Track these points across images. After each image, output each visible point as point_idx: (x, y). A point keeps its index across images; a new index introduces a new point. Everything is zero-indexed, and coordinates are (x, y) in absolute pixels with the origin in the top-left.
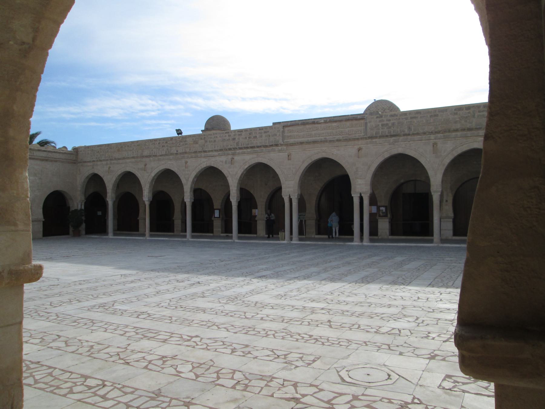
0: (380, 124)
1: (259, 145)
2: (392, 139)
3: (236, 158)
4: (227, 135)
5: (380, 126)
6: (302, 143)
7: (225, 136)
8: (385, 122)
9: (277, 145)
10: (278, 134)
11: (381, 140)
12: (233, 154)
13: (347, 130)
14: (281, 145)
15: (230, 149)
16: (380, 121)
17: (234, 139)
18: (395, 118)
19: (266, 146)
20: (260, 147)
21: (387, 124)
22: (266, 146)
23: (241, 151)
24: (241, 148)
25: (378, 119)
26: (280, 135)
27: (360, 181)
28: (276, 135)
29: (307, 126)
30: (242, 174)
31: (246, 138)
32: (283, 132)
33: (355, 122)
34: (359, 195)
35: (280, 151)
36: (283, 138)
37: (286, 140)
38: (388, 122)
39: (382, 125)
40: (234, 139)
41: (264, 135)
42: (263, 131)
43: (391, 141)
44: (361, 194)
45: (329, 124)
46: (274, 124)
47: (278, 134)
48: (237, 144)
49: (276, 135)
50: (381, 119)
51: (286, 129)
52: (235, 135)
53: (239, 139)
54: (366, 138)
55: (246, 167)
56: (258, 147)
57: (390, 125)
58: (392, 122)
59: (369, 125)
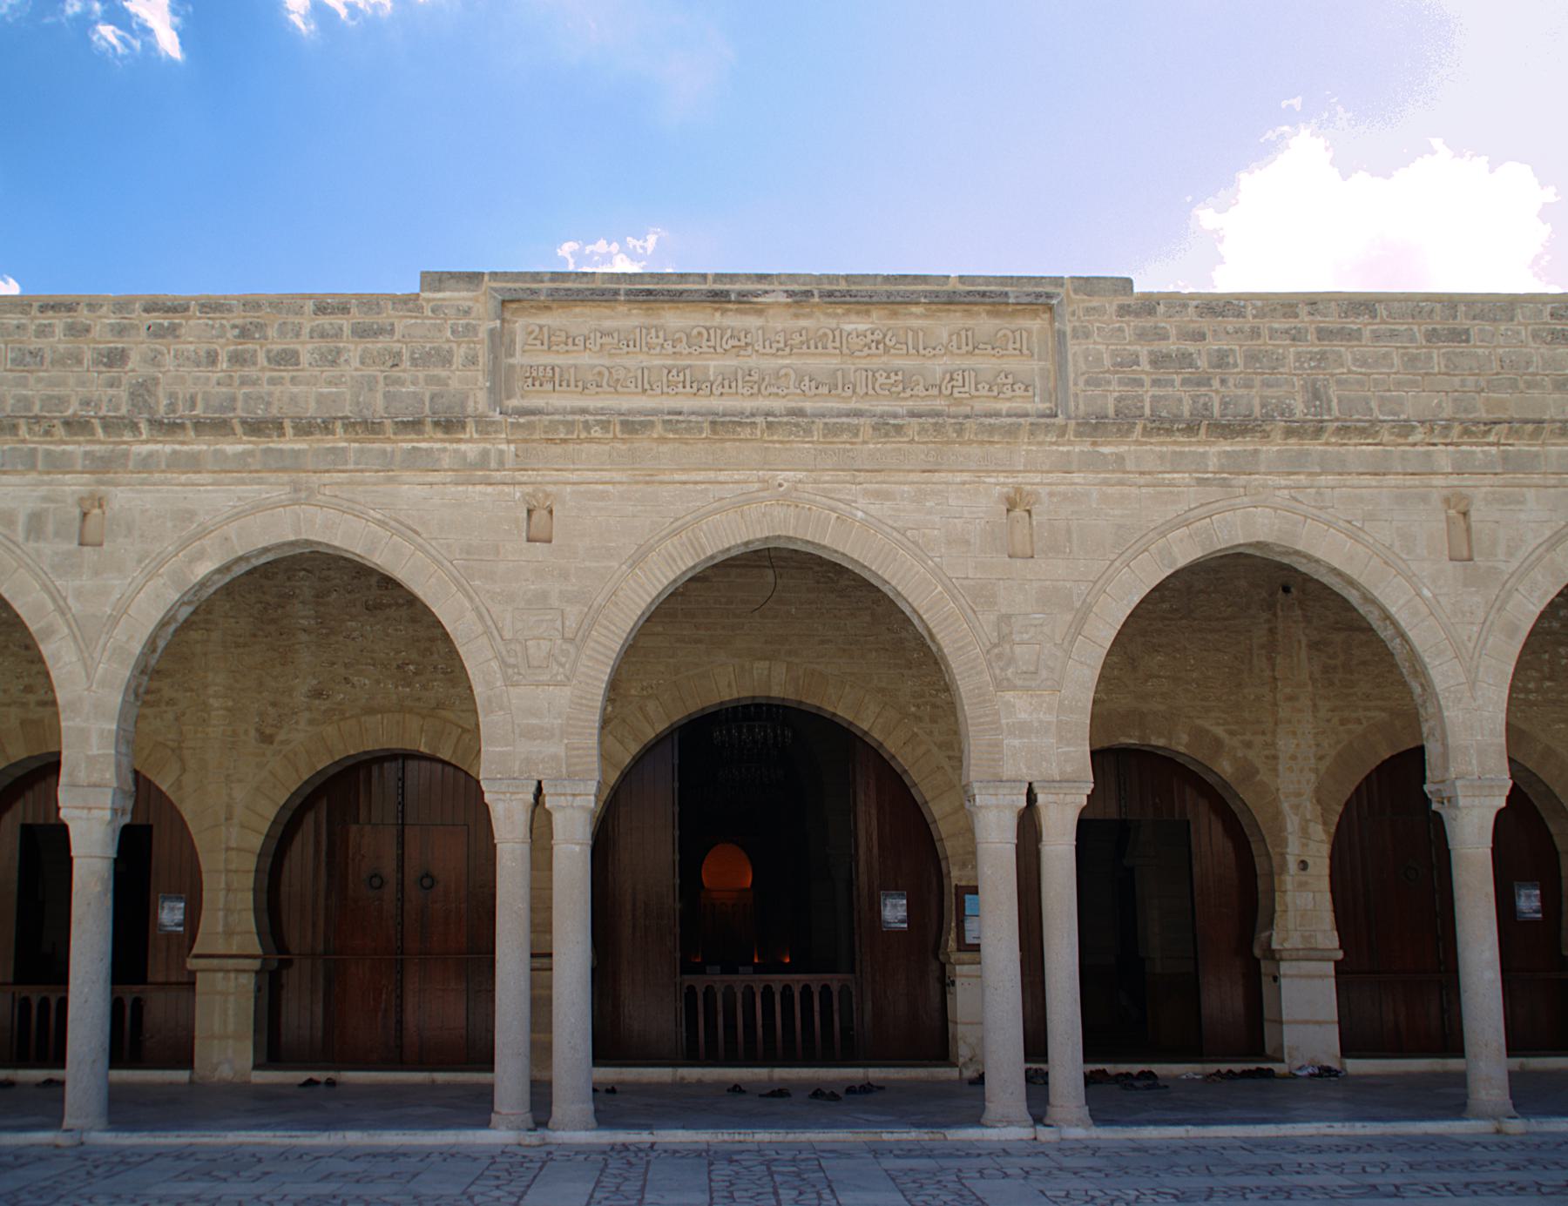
0: (1143, 351)
1: (311, 410)
3: (123, 497)
4: (59, 322)
7: (43, 331)
8: (1172, 346)
9: (450, 425)
10: (460, 353)
12: (102, 465)
13: (938, 366)
14: (485, 426)
15: (77, 426)
16: (1142, 335)
17: (115, 358)
18: (1231, 323)
21: (1185, 359)
22: (369, 427)
23: (165, 448)
24: (169, 428)
25: (1131, 325)
28: (446, 360)
29: (673, 319)
30: (163, 624)
31: (212, 358)
32: (500, 342)
33: (984, 324)
36: (501, 381)
38: (1191, 347)
39: (1158, 360)
40: (115, 358)
41: (353, 350)
42: (345, 323)
46: (435, 280)
47: (460, 353)
48: (142, 391)
49: (446, 360)
50: (1147, 322)
52: (121, 331)
53: (154, 360)
55: (203, 569)
56: (305, 428)
57: (1202, 363)
58: (1213, 345)
59: (1073, 347)
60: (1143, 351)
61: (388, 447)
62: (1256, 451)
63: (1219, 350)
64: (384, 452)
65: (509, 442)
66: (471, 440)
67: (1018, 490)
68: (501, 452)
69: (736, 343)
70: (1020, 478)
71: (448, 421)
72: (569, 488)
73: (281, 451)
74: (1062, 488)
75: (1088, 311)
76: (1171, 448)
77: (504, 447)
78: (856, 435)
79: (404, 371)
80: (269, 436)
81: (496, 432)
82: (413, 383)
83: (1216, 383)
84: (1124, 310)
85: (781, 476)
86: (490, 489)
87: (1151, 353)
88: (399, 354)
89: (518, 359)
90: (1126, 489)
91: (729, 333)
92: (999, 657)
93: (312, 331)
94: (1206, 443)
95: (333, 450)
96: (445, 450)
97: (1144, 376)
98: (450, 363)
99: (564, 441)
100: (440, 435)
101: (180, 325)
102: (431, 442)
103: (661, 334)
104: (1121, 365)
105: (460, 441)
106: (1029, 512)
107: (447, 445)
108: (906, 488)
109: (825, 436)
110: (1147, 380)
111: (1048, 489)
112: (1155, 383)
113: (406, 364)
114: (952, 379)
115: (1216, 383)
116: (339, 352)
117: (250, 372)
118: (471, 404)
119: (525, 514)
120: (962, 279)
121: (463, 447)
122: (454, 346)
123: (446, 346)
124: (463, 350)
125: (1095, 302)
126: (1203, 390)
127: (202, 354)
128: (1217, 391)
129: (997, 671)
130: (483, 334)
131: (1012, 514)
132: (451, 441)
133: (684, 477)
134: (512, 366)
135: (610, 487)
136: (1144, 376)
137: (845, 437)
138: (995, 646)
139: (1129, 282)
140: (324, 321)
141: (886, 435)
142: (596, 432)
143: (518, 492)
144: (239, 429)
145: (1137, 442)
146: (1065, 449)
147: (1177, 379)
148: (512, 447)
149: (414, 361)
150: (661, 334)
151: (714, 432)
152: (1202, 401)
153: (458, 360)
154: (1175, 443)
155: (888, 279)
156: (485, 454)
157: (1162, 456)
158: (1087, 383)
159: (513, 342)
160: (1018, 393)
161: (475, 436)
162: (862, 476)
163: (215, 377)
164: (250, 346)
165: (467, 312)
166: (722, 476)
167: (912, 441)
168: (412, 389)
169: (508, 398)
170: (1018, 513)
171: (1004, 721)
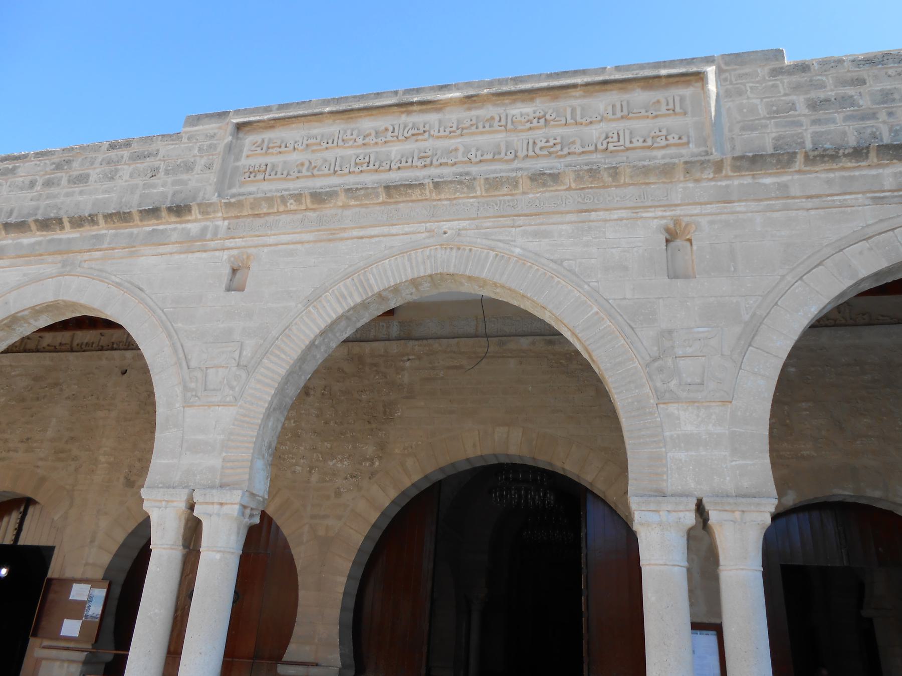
0: (800, 100)
5: (802, 108)
8: (830, 92)
9: (179, 210)
11: (820, 178)
13: (595, 132)
14: (206, 209)
16: (797, 88)
19: (121, 217)
20: (92, 220)
21: (845, 101)
26: (209, 167)
27: (688, 420)
28: (188, 167)
29: (367, 124)
31: (32, 184)
33: (639, 97)
35: (190, 244)
38: (850, 91)
39: (814, 105)
41: (125, 170)
42: (126, 153)
43: (889, 183)
51: (249, 140)
54: (718, 166)
56: (78, 222)
60: (800, 100)
61: (135, 231)
63: (881, 90)
64: (132, 234)
65: (224, 219)
66: (196, 221)
67: (677, 222)
68: (217, 228)
69: (416, 132)
70: (678, 212)
71: (178, 206)
72: (266, 250)
73: (60, 240)
74: (724, 217)
75: (740, 76)
76: (838, 174)
77: (220, 223)
78: (516, 186)
79: (159, 179)
80: (54, 230)
81: (214, 212)
82: (163, 186)
83: (882, 116)
84: (777, 72)
85: (446, 226)
86: (204, 255)
87: (808, 100)
88: (158, 169)
89: (244, 162)
90: (793, 214)
91: (410, 125)
92: (660, 370)
93: (103, 160)
94: (879, 166)
95: (96, 237)
96: (175, 229)
97: (802, 119)
98: (192, 169)
99: (268, 214)
100: (174, 219)
101: (19, 167)
102: (169, 225)
103: (355, 133)
104: (777, 112)
105: (188, 221)
106: (690, 241)
107: (178, 226)
108: (564, 227)
109: (487, 190)
111: (709, 218)
112: (815, 122)
113: (162, 174)
114: (607, 137)
115: (882, 116)
116: (117, 171)
117: (54, 190)
118: (201, 194)
119: (227, 271)
120: (618, 68)
121: (189, 226)
122: (198, 159)
123: (192, 160)
124: (204, 161)
125: (747, 70)
126: (869, 123)
127: (27, 182)
128: (884, 122)
129: (659, 384)
130: (221, 148)
131: (672, 244)
132: (181, 223)
133: (361, 233)
134: (237, 168)
135: (299, 246)
136: (802, 119)
137: (505, 190)
138: (655, 360)
139: (778, 54)
140: (113, 154)
141: (544, 185)
142: (292, 205)
143: (225, 255)
144: (33, 227)
145: (799, 172)
146: (724, 183)
147: (839, 117)
148: (226, 223)
149: (167, 172)
150: (355, 133)
151: (389, 195)
152: (869, 131)
153: (198, 168)
154: (843, 169)
156: (204, 230)
157: (829, 182)
158: (743, 129)
159: (241, 151)
160: (671, 141)
161: (199, 217)
162: (521, 221)
163: (30, 195)
164: (59, 174)
165: (212, 137)
166: (394, 230)
167: (569, 189)
168: (161, 189)
169: (230, 188)
170: (678, 243)
171: (667, 434)
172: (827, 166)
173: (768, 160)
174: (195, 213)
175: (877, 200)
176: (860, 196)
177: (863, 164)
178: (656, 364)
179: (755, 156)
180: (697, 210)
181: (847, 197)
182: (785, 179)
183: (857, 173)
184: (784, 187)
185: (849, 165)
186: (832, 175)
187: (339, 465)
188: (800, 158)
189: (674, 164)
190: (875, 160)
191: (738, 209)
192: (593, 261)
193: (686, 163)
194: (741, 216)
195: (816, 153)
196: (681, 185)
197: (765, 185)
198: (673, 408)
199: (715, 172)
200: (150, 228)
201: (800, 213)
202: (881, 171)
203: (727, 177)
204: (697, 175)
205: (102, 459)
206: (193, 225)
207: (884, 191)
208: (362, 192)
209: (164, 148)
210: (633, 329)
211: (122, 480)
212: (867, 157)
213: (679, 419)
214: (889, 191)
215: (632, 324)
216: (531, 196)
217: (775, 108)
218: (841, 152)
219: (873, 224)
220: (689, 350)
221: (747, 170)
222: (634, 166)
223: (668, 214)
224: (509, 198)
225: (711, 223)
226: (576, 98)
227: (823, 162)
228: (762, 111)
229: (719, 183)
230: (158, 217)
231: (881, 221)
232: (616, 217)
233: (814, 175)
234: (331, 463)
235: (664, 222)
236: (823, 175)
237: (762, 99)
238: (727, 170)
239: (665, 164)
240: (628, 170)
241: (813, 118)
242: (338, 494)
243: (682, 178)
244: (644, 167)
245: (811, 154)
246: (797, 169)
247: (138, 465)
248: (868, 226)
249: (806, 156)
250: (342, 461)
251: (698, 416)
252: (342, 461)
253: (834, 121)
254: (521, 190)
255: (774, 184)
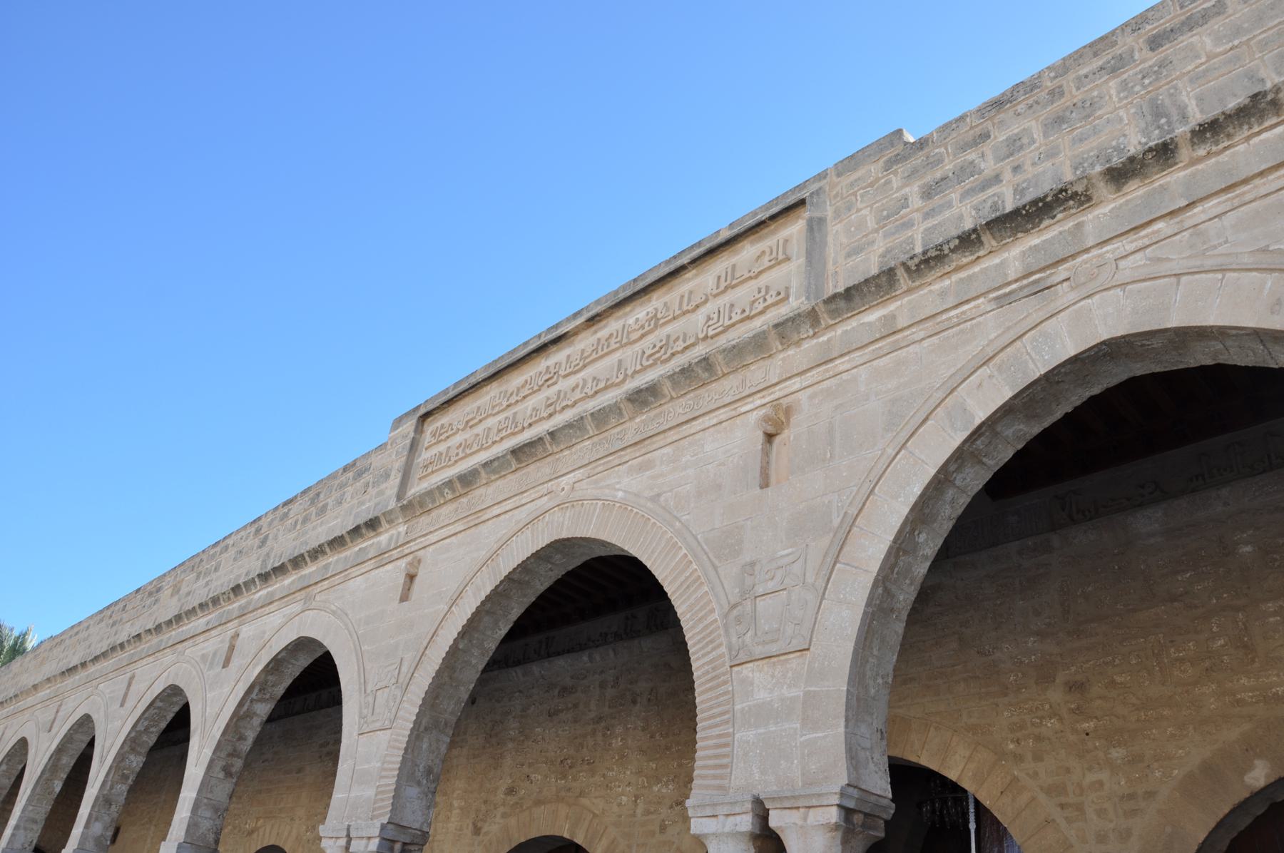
2: (1012, 257)
6: (467, 480)
11: (934, 291)
27: (761, 685)
34: (746, 823)
35: (382, 558)
37: (413, 491)
44: (762, 815)
45: (612, 326)
62: (1079, 226)
66: (386, 531)
70: (777, 392)
76: (955, 277)
78: (621, 414)
83: (1007, 175)
92: (738, 620)
104: (888, 217)
108: (665, 451)
109: (597, 427)
110: (917, 216)
119: (401, 579)
120: (731, 226)
138: (734, 607)
143: (402, 563)
145: (909, 291)
146: (824, 338)
151: (519, 460)
154: (959, 269)
155: (668, 262)
157: (943, 294)
167: (672, 398)
172: (939, 272)
173: (865, 290)
174: (385, 525)
175: (1002, 301)
176: (981, 300)
177: (981, 253)
178: (735, 612)
179: (848, 290)
180: (796, 384)
181: (966, 307)
182: (892, 307)
183: (977, 269)
184: (892, 317)
185: (965, 260)
186: (947, 282)
187: (664, 791)
188: (901, 273)
189: (764, 332)
190: (994, 243)
191: (842, 368)
192: (688, 487)
193: (776, 326)
194: (844, 376)
195: (916, 260)
196: (781, 356)
197: (869, 324)
198: (746, 670)
199: (812, 326)
200: (357, 549)
201: (911, 349)
202: (1006, 255)
203: (828, 327)
204: (795, 337)
205: (456, 803)
206: (383, 538)
207: (1009, 284)
208: (496, 464)
209: (376, 461)
210: (715, 568)
211: (471, 826)
212: (981, 243)
213: (752, 684)
214: (1016, 281)
215: (716, 562)
216: (638, 420)
217: (885, 213)
218: (946, 248)
219: (999, 336)
220: (771, 585)
221: (848, 310)
222: (724, 350)
223: (767, 399)
224: (619, 429)
225: (811, 397)
226: (689, 280)
227: (931, 268)
228: (871, 224)
229: (821, 339)
230: (361, 536)
231: (1009, 328)
232: (715, 421)
233: (926, 291)
234: (656, 789)
235: (762, 412)
236: (936, 287)
237: (871, 206)
238: (825, 320)
239: (754, 336)
240: (720, 357)
241: (926, 209)
242: (663, 828)
243: (780, 347)
244: (734, 347)
245: (910, 263)
246: (905, 288)
247: (483, 808)
248: (992, 341)
249: (908, 269)
250: (666, 785)
251: (773, 676)
252: (666, 785)
253: (949, 205)
254: (627, 418)
255: (880, 319)
